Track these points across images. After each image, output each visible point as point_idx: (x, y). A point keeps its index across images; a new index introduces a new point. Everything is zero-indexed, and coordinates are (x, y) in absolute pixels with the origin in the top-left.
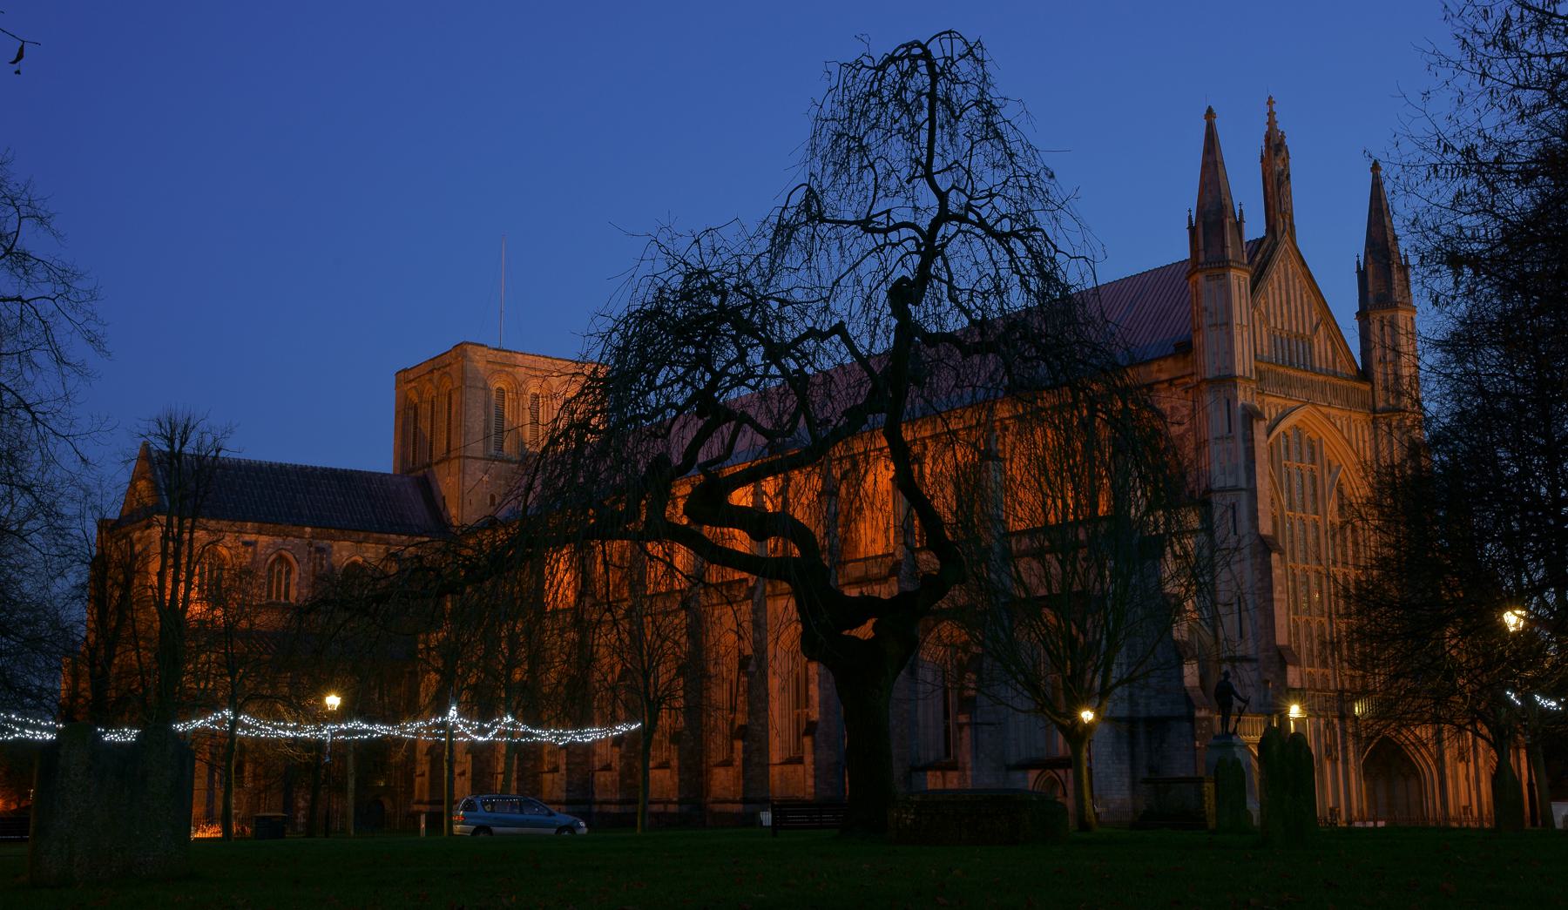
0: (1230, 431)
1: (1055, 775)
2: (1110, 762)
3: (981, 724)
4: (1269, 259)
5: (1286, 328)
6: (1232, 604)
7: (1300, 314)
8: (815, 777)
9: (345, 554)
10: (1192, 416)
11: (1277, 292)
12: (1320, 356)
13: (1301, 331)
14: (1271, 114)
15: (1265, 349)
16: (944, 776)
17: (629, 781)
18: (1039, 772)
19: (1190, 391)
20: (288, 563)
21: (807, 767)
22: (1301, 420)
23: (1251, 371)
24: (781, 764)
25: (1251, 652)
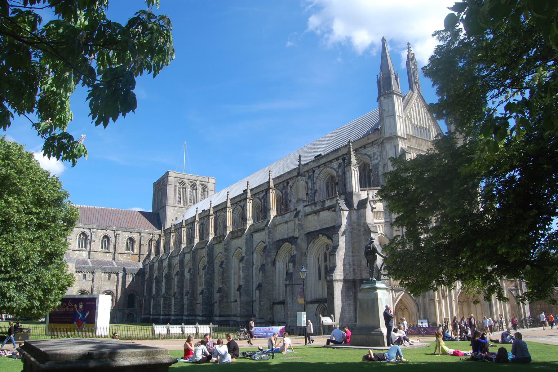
1: (324, 306)
3: (295, 284)
4: (411, 97)
5: (419, 124)
7: (424, 120)
8: (240, 307)
9: (127, 235)
10: (380, 155)
11: (415, 111)
13: (425, 126)
15: (411, 131)
17: (190, 308)
18: (318, 304)
19: (380, 145)
21: (238, 303)
23: (404, 134)
24: (234, 302)
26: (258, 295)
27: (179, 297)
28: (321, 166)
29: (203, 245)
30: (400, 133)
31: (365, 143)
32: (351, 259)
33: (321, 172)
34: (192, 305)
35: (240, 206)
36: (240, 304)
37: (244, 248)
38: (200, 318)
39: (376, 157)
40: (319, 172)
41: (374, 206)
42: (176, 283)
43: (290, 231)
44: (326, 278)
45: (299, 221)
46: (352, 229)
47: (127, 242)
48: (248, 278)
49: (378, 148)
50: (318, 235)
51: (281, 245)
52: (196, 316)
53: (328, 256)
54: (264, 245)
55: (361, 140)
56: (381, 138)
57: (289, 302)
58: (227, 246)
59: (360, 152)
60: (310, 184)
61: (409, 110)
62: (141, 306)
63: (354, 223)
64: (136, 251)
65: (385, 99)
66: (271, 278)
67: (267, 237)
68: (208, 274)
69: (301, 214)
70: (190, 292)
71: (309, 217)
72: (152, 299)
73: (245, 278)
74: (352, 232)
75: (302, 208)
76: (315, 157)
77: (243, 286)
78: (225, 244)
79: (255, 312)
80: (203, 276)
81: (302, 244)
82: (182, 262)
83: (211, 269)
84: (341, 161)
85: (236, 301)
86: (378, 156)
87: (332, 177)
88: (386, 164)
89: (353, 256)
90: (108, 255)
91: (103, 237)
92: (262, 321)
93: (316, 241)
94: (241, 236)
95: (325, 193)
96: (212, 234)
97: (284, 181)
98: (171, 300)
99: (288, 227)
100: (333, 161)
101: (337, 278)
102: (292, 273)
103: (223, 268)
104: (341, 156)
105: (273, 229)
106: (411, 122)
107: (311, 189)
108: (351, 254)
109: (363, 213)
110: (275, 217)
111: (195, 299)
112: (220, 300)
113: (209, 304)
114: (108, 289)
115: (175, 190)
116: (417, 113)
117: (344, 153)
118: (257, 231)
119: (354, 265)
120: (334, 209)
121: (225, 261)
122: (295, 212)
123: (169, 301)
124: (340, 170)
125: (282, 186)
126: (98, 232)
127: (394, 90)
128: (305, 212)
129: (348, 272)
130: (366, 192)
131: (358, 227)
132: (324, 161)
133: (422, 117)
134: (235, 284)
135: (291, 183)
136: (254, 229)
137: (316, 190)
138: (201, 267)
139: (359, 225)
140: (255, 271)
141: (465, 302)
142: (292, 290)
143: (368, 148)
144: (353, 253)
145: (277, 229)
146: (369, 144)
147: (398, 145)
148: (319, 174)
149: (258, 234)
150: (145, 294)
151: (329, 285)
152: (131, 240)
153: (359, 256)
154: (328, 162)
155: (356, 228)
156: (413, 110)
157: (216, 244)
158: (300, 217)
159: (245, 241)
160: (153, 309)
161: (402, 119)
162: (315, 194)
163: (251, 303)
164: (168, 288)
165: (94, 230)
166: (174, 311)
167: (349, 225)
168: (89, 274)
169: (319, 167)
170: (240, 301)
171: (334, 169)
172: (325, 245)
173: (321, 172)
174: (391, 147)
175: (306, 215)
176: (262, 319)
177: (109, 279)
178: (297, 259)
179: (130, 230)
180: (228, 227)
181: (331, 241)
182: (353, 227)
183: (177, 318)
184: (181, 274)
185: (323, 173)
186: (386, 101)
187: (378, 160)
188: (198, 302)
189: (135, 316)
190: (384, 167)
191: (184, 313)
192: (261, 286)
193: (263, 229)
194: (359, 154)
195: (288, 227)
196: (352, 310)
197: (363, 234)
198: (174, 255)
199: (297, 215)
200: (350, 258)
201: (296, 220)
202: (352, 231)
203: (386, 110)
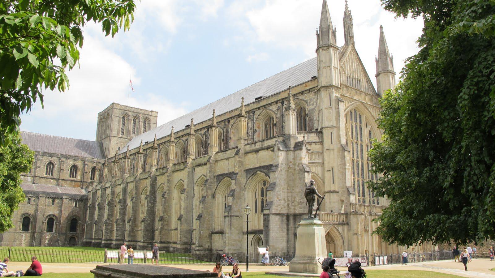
0: (330, 105)
2: (278, 232)
3: (233, 216)
6: (330, 171)
8: (181, 235)
12: (363, 87)
14: (346, 5)
16: (222, 235)
17: (132, 234)
18: (254, 235)
19: (317, 92)
20: (53, 164)
22: (356, 107)
23: (338, 84)
24: (174, 230)
25: (337, 190)
26: (198, 224)
27: (121, 224)
28: (261, 108)
29: (146, 176)
30: (335, 82)
31: (303, 90)
32: (286, 195)
33: (261, 113)
34: (133, 231)
35: (182, 140)
36: (181, 232)
37: (186, 182)
38: (141, 244)
39: (311, 103)
40: (259, 113)
41: (309, 148)
42: (118, 210)
43: (231, 167)
44: (262, 211)
45: (239, 158)
46: (289, 168)
47: (71, 169)
48: (189, 209)
49: (315, 95)
50: (257, 172)
51: (222, 180)
52: (137, 241)
53: (265, 191)
54: (206, 178)
55: (299, 87)
56: (317, 86)
57: (227, 232)
58: (170, 177)
59: (297, 98)
60: (250, 124)
61: (343, 62)
62: (83, 230)
63: (290, 162)
64: (79, 178)
65: (323, 51)
66: (210, 210)
67: (208, 172)
68: (150, 202)
69: (242, 152)
70: (132, 219)
71: (249, 154)
72: (94, 225)
73: (186, 208)
74: (288, 171)
75: (243, 147)
76: (256, 99)
77: (184, 216)
78: (168, 176)
79: (194, 240)
80: (146, 205)
81: (242, 179)
82: (125, 190)
83: (153, 198)
84: (280, 104)
85: (176, 229)
86: (314, 102)
87: (271, 118)
88: (321, 110)
89: (288, 193)
90: (52, 180)
91: (48, 164)
92: (201, 248)
93: (254, 178)
94: (184, 169)
95: (264, 133)
96: (155, 165)
97: (226, 120)
98: (112, 225)
99: (228, 164)
100: (273, 104)
101: (273, 212)
102: (231, 206)
103: (165, 198)
104: (279, 100)
105: (215, 164)
106: (345, 73)
107: (251, 129)
108: (286, 190)
109: (299, 154)
110: (217, 153)
111: (136, 226)
112: (161, 228)
113: (150, 231)
114: (51, 213)
115: (119, 121)
117: (283, 97)
118: (199, 165)
119: (288, 201)
120: (272, 149)
121: (167, 191)
122: (236, 150)
123: (110, 227)
124: (279, 113)
125: (223, 124)
126: (43, 159)
127: (331, 43)
128: (245, 150)
129: (283, 207)
130: (302, 135)
131: (293, 166)
132: (263, 103)
133: (355, 69)
134: (176, 213)
135: (232, 122)
136: (196, 163)
137: (256, 130)
138: (143, 197)
139: (294, 165)
140: (196, 202)
142: (231, 221)
143: (305, 94)
144: (288, 189)
145: (218, 164)
146: (306, 91)
147: (333, 93)
148: (259, 115)
149: (200, 168)
150: (87, 219)
151: (265, 219)
152: (74, 168)
153: (293, 192)
154: (267, 105)
155: (292, 167)
156: (347, 62)
157: (159, 175)
158: (240, 154)
159: (187, 174)
160: (95, 234)
161: (338, 70)
162: (254, 133)
163: (191, 232)
164: (111, 215)
165: (40, 157)
166: (116, 236)
167: (285, 165)
168: (33, 199)
169: (259, 108)
170: (181, 230)
171: (273, 112)
172: (262, 182)
173: (261, 113)
174: (326, 94)
175: (247, 153)
176: (202, 246)
177: (53, 204)
178: (236, 193)
179: (75, 158)
180: (171, 160)
181: (268, 178)
182: (290, 166)
183: (119, 243)
184: (123, 202)
185: (262, 114)
186: (324, 52)
187: (314, 106)
188: (140, 229)
189: (76, 239)
190: (319, 113)
191: (126, 239)
192: (201, 216)
193: (205, 164)
194: (297, 99)
195: (228, 164)
196: (285, 241)
197: (298, 173)
198: (117, 184)
199: (237, 153)
201: (237, 157)
202: (288, 169)
203: (323, 61)
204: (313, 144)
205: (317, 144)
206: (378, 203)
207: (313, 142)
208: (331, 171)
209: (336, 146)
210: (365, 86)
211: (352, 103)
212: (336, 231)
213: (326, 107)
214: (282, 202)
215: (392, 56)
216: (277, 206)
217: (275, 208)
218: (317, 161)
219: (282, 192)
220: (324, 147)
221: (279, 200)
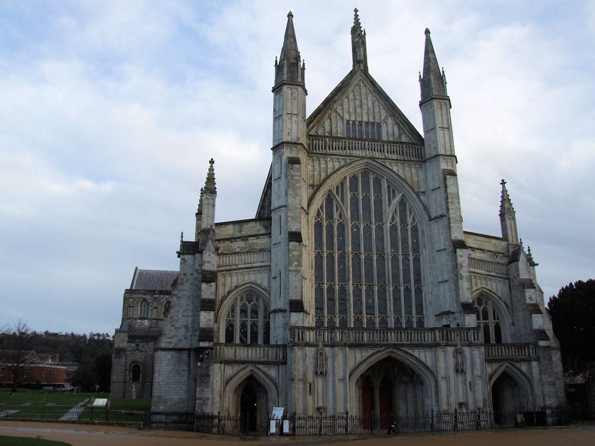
6: (276, 277)
14: (356, 16)
22: (366, 168)
32: (190, 320)
91: (166, 304)
106: (342, 118)
108: (190, 313)
116: (358, 103)
129: (183, 338)
141: (410, 382)
155: (197, 278)
165: (156, 296)
200: (188, 319)
204: (252, 238)
205: (261, 237)
206: (421, 322)
207: (250, 236)
208: (278, 278)
209: (284, 237)
210: (393, 130)
211: (349, 162)
212: (261, 374)
213: (276, 178)
214: (182, 331)
215: (443, 72)
216: (170, 338)
217: (167, 340)
218: (261, 264)
219: (183, 316)
220: (272, 240)
221: (176, 328)
